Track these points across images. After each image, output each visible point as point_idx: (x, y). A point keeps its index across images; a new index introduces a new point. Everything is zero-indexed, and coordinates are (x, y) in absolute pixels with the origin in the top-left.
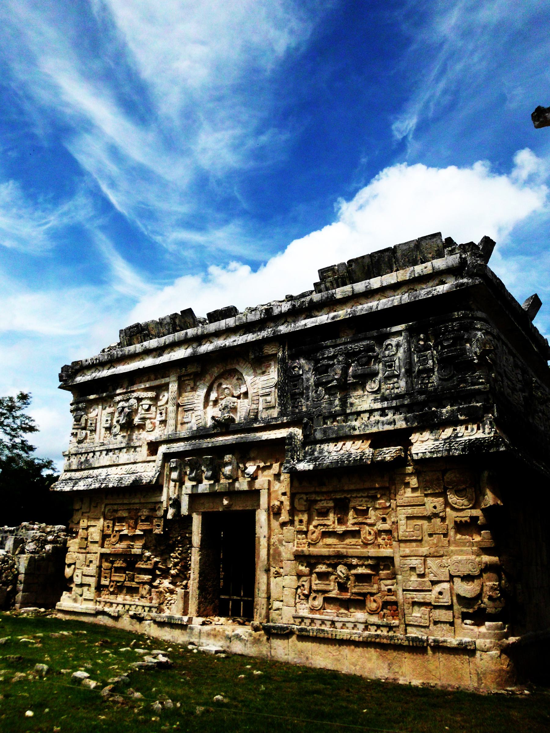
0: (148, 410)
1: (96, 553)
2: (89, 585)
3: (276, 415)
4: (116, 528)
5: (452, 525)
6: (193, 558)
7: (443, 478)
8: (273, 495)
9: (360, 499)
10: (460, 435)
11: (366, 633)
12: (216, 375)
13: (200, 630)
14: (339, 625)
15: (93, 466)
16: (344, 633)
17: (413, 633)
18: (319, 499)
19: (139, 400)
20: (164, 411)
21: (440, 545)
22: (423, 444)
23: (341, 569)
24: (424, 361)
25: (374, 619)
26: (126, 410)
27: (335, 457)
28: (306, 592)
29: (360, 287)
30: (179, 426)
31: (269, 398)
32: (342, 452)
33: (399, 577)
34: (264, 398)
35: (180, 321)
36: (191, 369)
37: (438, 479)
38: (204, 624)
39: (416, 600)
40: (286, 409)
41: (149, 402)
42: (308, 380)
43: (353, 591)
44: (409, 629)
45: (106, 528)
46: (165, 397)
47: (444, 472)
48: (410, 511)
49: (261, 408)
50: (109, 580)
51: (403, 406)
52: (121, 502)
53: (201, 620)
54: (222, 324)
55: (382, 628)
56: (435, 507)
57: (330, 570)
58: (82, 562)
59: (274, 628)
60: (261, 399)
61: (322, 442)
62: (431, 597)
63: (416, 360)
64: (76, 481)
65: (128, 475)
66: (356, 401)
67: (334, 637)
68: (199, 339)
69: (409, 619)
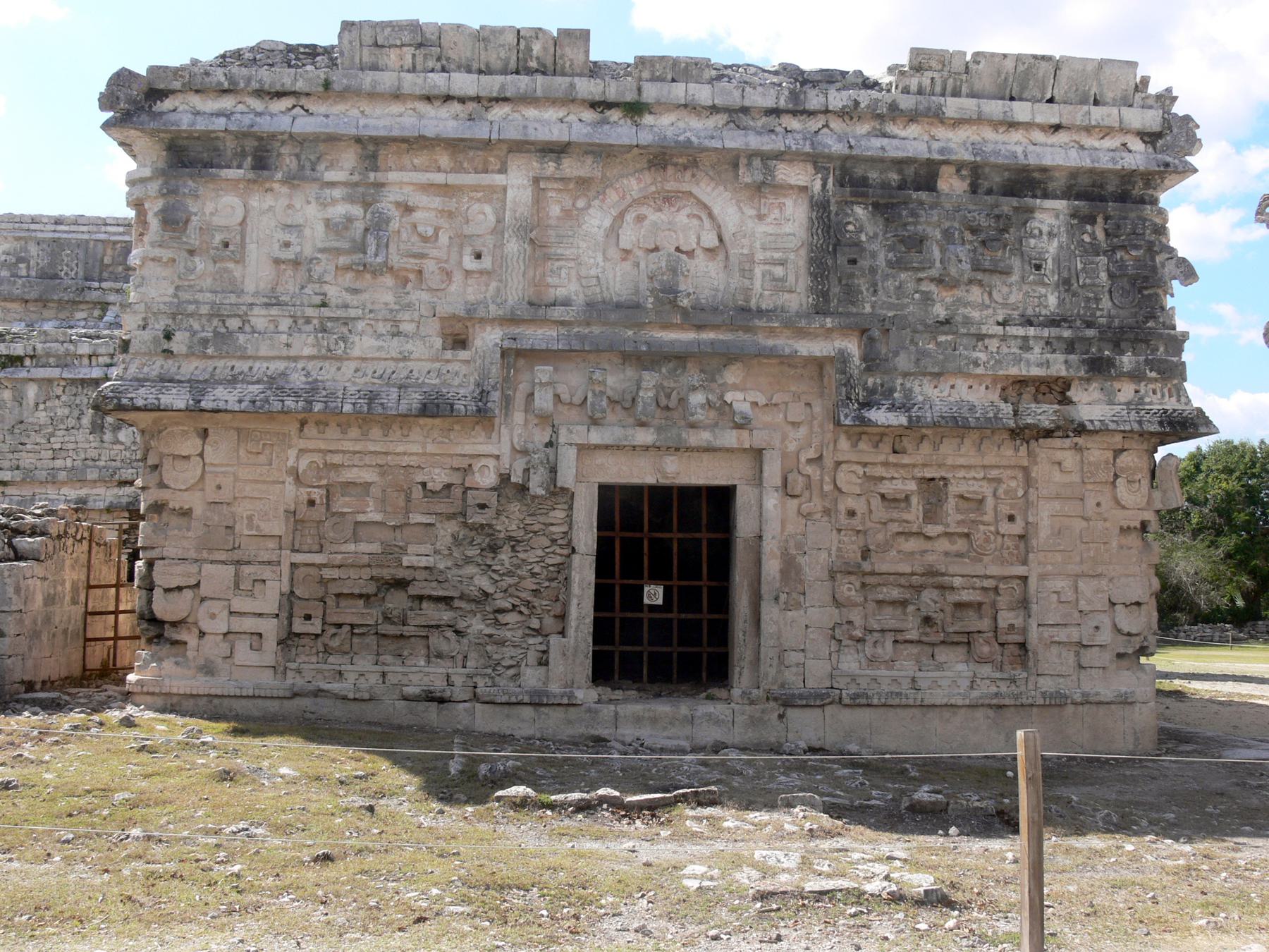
6: (576, 577)
7: (1115, 459)
9: (970, 482)
10: (1147, 400)
11: (975, 694)
12: (635, 195)
13: (616, 713)
14: (922, 684)
15: (249, 353)
16: (939, 697)
17: (1047, 684)
18: (889, 476)
20: (485, 251)
22: (1090, 405)
23: (928, 596)
24: (1091, 271)
25: (986, 670)
31: (779, 271)
33: (1034, 607)
34: (767, 267)
35: (545, 49)
36: (571, 167)
37: (1107, 462)
39: (1056, 639)
42: (874, 255)
43: (951, 630)
44: (1041, 680)
45: (303, 508)
46: (483, 215)
47: (1118, 452)
48: (1057, 505)
51: (1059, 338)
52: (358, 448)
54: (679, 91)
56: (1098, 504)
57: (908, 596)
59: (801, 697)
61: (906, 375)
63: (1080, 266)
66: (976, 315)
67: (918, 703)
69: (1044, 667)
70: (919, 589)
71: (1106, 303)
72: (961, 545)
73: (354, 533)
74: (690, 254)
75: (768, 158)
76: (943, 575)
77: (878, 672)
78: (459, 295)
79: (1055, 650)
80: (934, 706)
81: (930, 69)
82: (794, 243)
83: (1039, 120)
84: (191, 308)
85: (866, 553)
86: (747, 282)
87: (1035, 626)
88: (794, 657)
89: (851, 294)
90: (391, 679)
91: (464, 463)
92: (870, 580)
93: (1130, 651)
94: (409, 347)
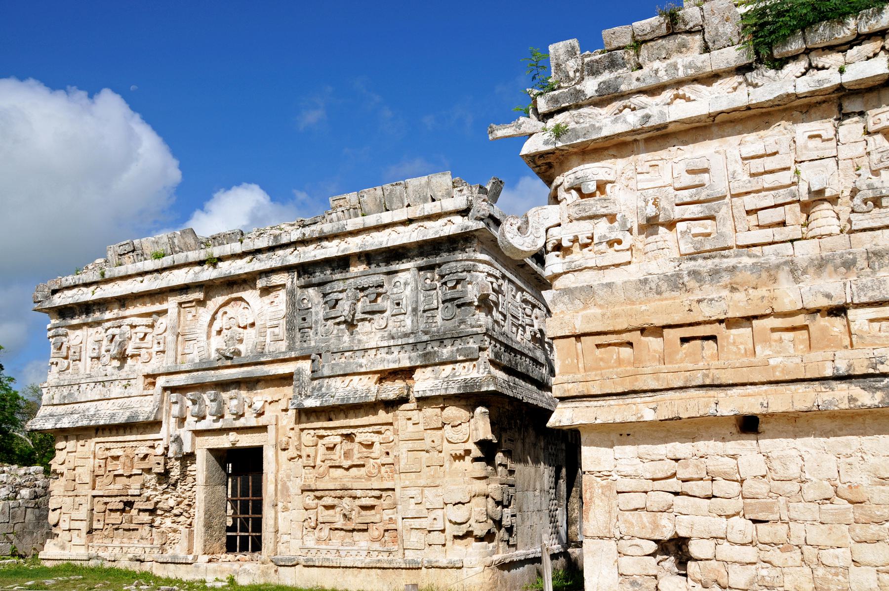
0: (143, 339)
3: (284, 350)
4: (109, 468)
5: (448, 457)
6: (197, 497)
8: (280, 431)
10: (457, 374)
14: (343, 554)
17: (410, 555)
19: (133, 327)
20: (161, 341)
21: (437, 475)
25: (377, 546)
26: (117, 338)
27: (342, 394)
28: (313, 525)
29: (371, 220)
30: (179, 357)
31: (276, 330)
32: (348, 388)
33: (399, 507)
35: (179, 241)
38: (210, 561)
39: (413, 527)
40: (294, 343)
41: (144, 329)
42: (317, 314)
47: (443, 409)
48: (411, 445)
49: (268, 340)
50: (102, 523)
53: (206, 558)
55: (383, 554)
58: (68, 506)
59: (282, 560)
60: (269, 331)
61: (329, 377)
62: (425, 523)
64: (60, 417)
65: (122, 411)
66: (364, 338)
68: (201, 263)
71: (439, 318)
73: (114, 479)
74: (245, 328)
77: (320, 547)
79: (414, 532)
80: (346, 567)
81: (341, 206)
82: (283, 313)
83: (396, 219)
84: (62, 383)
86: (262, 339)
87: (400, 519)
88: (285, 538)
90: (125, 550)
91: (150, 443)
92: (318, 494)
93: (461, 534)
94: (131, 391)
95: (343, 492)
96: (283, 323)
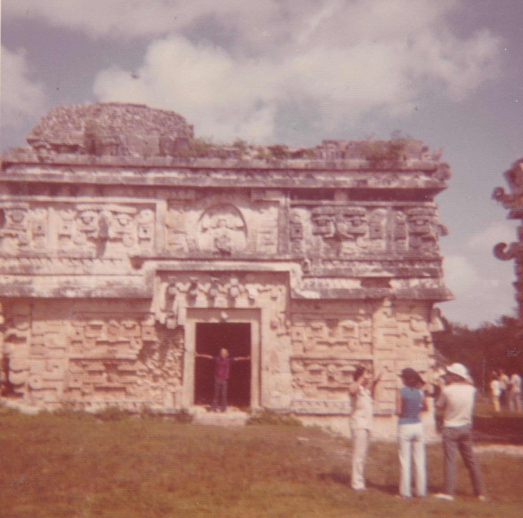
1: (63, 358)
2: (55, 389)
19: (115, 213)
23: (332, 368)
31: (268, 236)
46: (147, 215)
51: (386, 261)
70: (326, 365)
72: (344, 348)
75: (263, 190)
76: (338, 359)
78: (138, 250)
85: (305, 350)
89: (297, 246)
95: (326, 362)
96: (276, 231)
